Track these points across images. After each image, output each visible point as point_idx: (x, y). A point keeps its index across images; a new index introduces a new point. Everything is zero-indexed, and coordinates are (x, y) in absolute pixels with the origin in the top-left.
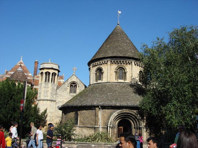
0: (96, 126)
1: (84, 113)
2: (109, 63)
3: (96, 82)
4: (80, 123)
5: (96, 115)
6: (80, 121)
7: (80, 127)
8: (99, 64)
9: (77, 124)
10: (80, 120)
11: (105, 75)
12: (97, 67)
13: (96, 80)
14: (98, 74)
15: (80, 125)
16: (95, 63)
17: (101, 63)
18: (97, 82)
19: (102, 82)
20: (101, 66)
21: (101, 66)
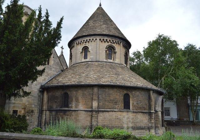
0: (152, 111)
1: (138, 96)
2: (122, 44)
3: (106, 61)
4: (133, 107)
5: (150, 98)
6: (133, 105)
7: (133, 112)
8: (111, 41)
9: (129, 109)
10: (133, 103)
11: (118, 55)
12: (106, 44)
13: (107, 58)
14: (108, 52)
15: (133, 110)
16: (106, 38)
17: (114, 42)
18: (107, 61)
19: (115, 62)
20: (113, 45)
21: (113, 45)
